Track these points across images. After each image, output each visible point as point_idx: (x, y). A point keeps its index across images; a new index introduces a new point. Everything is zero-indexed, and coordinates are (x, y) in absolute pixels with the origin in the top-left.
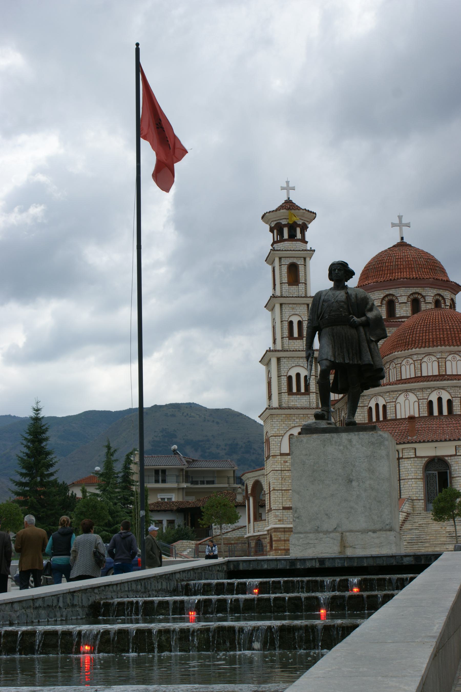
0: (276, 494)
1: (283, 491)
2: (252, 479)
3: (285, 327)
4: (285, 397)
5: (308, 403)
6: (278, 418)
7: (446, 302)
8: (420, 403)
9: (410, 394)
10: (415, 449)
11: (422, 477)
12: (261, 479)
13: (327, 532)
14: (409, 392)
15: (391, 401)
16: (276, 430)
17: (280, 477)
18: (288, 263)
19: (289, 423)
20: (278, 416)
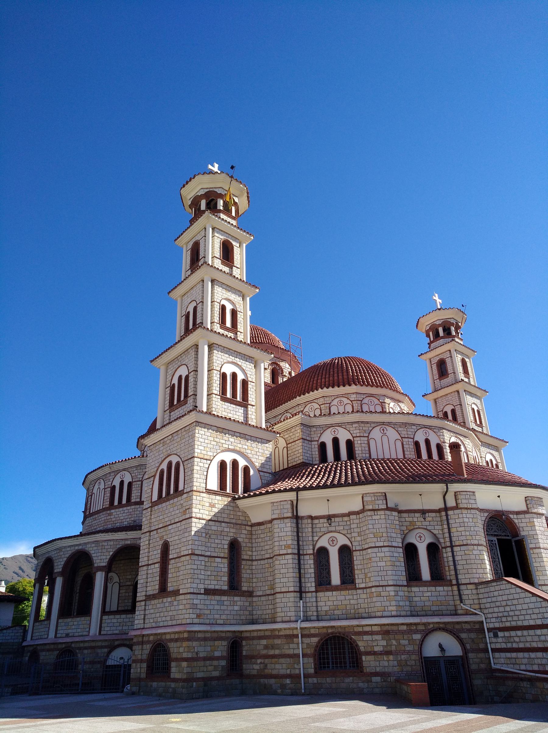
0: (196, 562)
8: (404, 443)
9: (389, 429)
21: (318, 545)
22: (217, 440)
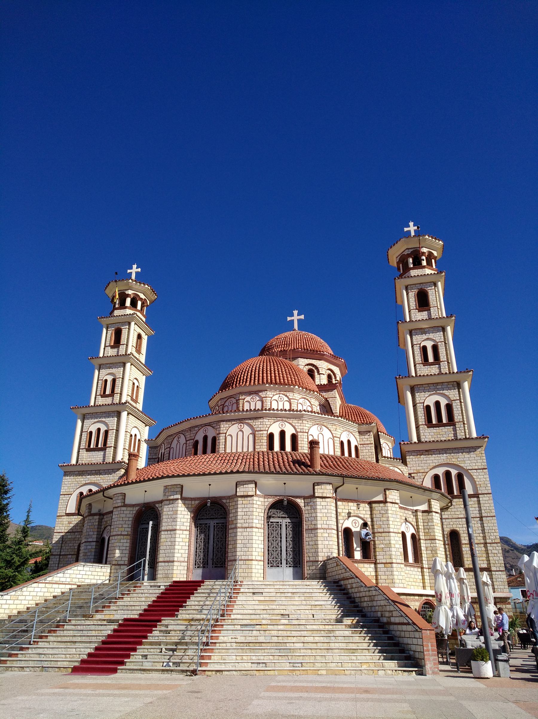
11: (130, 533)
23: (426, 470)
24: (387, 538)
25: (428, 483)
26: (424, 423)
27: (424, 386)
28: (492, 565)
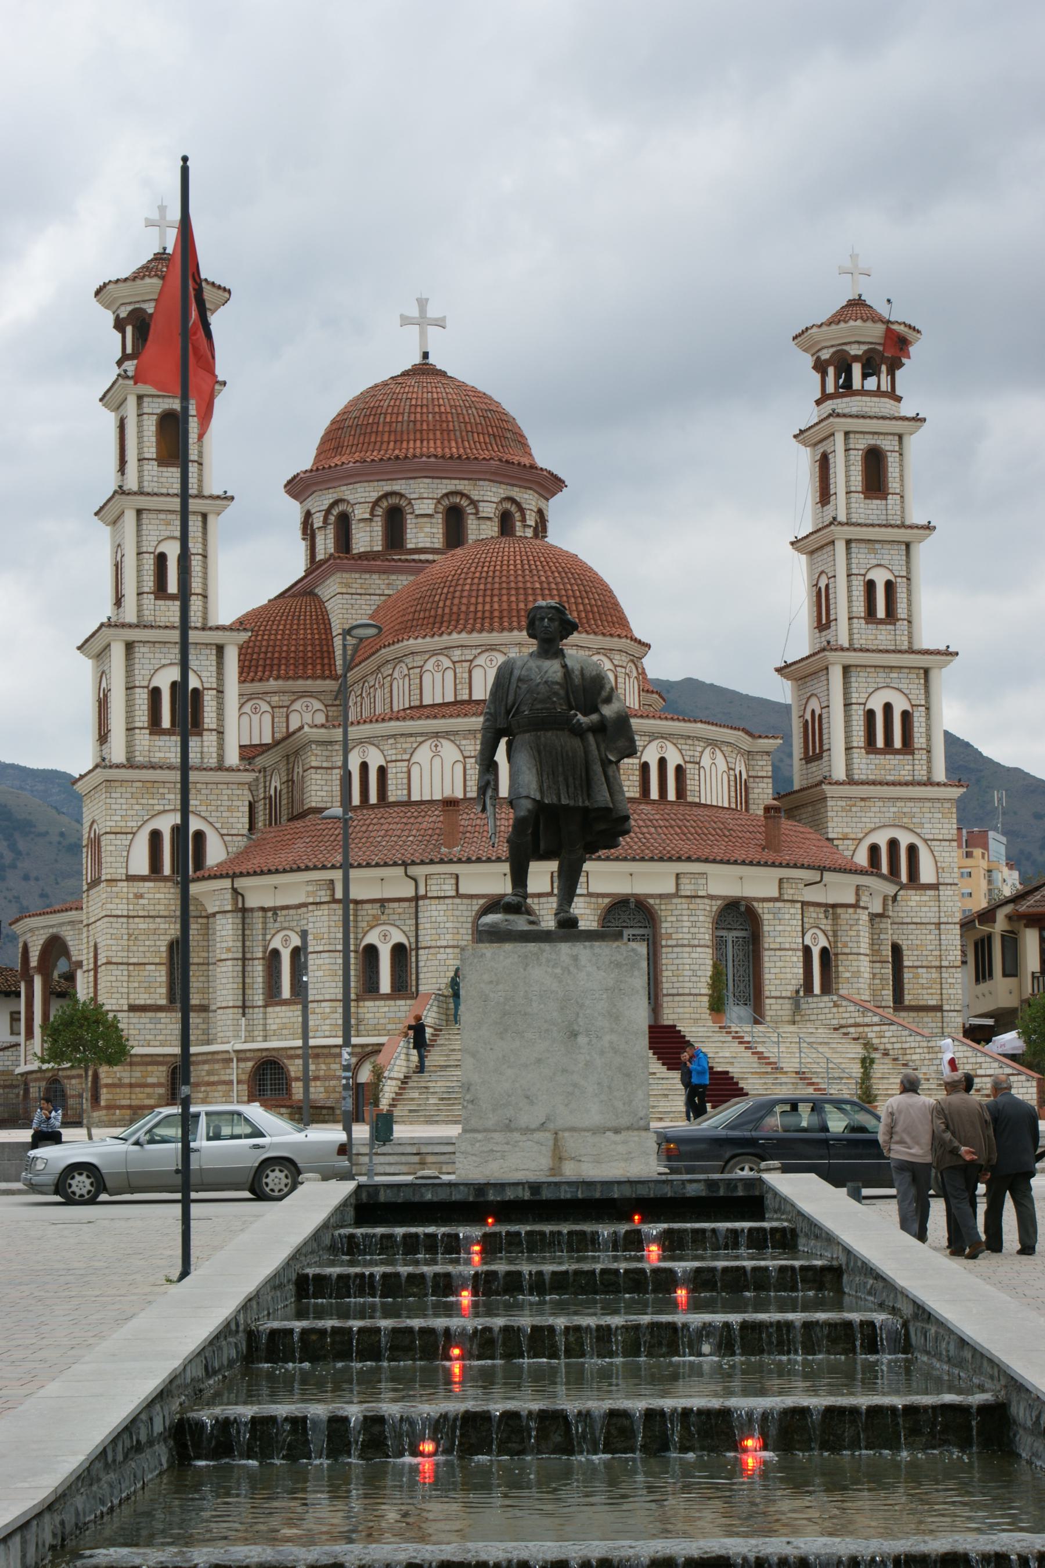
0: (115, 973)
1: (131, 968)
2: (42, 932)
3: (146, 567)
4: (143, 739)
5: (199, 755)
6: (124, 790)
7: (527, 517)
9: (444, 742)
10: (457, 877)
12: (67, 933)
13: (527, 1131)
14: (443, 737)
15: (399, 757)
16: (119, 818)
17: (125, 931)
18: (159, 411)
19: (151, 802)
20: (125, 784)
21: (271, 947)
22: (144, 801)
23: (861, 836)
24: (855, 964)
25: (862, 858)
26: (862, 744)
27: (868, 670)
28: (945, 1002)
